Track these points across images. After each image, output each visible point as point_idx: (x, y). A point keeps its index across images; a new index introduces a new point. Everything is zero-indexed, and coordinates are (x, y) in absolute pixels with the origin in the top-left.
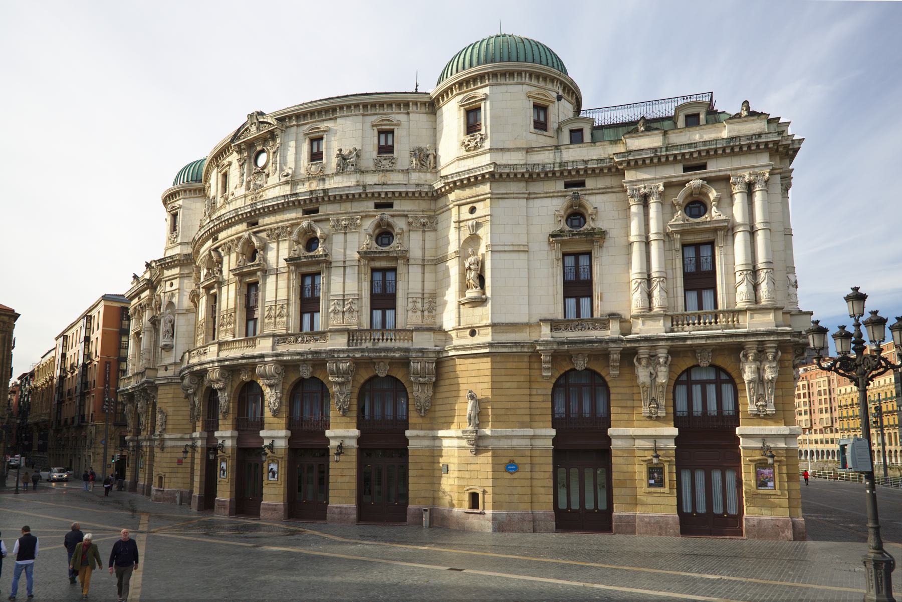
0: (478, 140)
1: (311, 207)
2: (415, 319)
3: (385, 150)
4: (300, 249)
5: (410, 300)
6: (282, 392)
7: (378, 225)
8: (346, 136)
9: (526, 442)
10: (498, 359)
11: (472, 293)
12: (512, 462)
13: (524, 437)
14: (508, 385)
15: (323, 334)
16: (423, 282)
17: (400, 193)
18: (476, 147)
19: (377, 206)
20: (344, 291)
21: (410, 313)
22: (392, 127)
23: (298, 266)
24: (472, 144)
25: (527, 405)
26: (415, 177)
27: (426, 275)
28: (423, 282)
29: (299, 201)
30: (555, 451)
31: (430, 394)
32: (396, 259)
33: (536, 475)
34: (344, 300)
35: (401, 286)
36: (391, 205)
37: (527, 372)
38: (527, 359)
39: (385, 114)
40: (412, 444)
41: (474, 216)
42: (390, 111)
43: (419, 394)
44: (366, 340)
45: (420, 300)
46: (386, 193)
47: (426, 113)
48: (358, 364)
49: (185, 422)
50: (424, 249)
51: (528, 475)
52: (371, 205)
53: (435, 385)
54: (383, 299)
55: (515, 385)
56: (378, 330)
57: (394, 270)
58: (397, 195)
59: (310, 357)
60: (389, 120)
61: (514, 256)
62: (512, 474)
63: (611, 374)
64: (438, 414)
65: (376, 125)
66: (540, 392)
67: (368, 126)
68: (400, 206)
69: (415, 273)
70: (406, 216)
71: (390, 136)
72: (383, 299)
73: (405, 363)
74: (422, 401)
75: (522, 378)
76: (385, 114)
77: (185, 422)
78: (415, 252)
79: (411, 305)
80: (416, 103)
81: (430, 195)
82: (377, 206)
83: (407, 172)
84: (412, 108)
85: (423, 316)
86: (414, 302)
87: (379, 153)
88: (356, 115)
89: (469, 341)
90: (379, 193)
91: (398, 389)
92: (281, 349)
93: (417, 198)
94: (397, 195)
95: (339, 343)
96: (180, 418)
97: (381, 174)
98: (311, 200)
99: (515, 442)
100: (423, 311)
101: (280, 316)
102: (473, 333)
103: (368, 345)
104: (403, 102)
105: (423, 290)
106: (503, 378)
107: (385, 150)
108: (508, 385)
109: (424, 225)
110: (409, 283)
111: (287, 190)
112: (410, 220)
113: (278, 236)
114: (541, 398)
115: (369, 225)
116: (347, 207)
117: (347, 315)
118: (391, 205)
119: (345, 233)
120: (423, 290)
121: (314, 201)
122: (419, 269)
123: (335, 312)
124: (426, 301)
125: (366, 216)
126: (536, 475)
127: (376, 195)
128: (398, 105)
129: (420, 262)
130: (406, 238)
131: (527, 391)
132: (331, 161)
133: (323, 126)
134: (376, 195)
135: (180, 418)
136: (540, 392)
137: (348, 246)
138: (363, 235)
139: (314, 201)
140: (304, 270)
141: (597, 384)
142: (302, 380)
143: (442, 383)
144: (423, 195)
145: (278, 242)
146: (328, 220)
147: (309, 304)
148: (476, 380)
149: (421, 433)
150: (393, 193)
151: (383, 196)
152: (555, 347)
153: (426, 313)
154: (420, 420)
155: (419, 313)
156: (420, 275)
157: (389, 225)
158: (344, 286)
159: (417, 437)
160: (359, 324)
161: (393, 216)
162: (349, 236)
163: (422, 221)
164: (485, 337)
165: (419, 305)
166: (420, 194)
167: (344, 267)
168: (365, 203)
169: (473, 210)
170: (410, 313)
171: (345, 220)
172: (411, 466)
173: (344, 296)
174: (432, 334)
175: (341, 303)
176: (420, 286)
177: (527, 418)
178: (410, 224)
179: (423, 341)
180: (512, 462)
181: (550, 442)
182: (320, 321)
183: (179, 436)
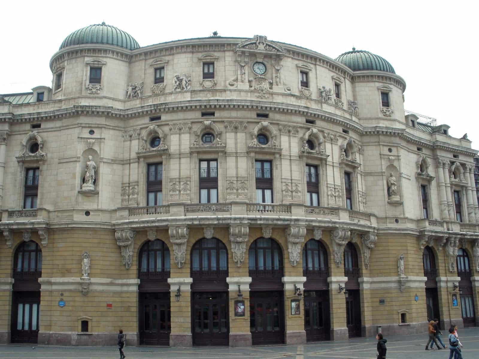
0: (390, 112)
1: (311, 119)
49: (113, 267)
65: (335, 79)
76: (336, 73)
77: (113, 267)
88: (326, 68)
89: (394, 226)
96: (108, 263)
97: (342, 112)
102: (397, 221)
110: (360, 185)
119: (332, 144)
135: (108, 263)
148: (399, 248)
169: (390, 150)
175: (333, 190)
183: (108, 280)
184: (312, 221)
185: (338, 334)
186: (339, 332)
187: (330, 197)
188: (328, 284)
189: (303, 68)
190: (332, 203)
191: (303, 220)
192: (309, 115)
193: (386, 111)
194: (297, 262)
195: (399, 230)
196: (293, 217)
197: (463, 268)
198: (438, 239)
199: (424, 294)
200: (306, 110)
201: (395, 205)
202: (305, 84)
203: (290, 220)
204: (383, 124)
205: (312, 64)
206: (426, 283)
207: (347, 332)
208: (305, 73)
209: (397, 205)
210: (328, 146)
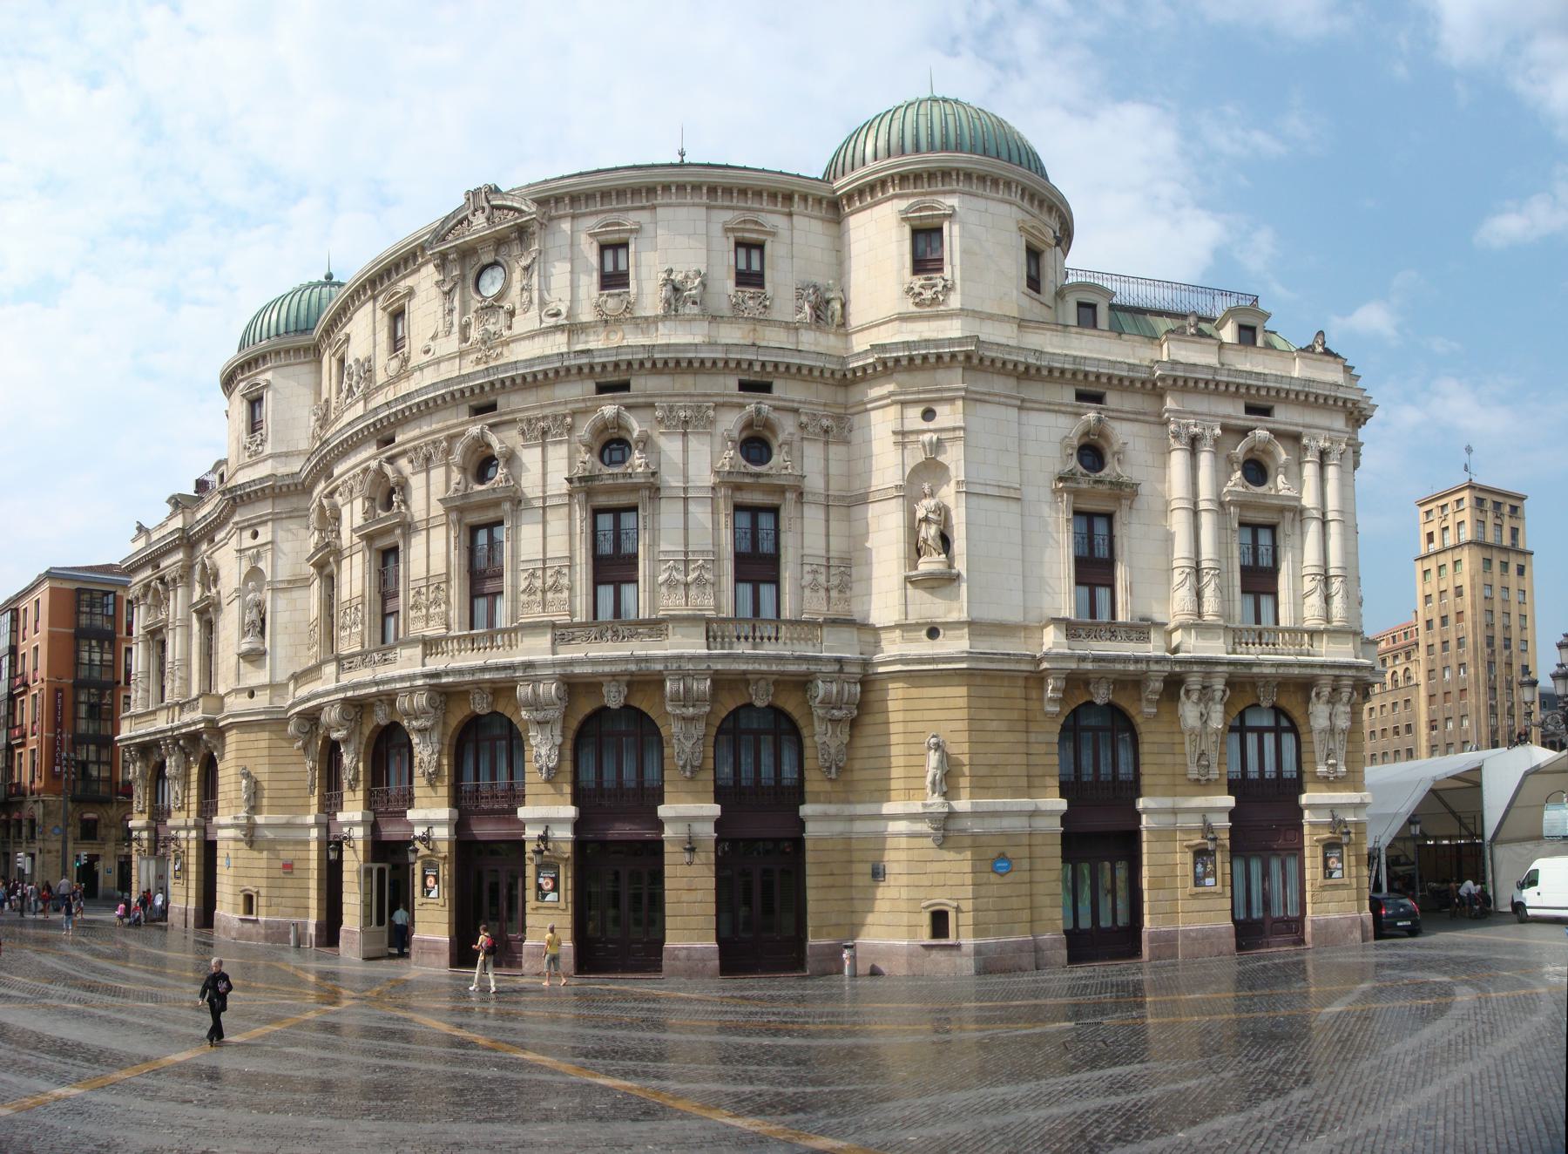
0: (940, 288)
2: (816, 606)
3: (749, 279)
4: (586, 460)
5: (807, 568)
6: (563, 735)
7: (749, 425)
8: (676, 247)
9: (1019, 824)
10: (978, 681)
11: (931, 563)
12: (1002, 857)
13: (1019, 813)
14: (994, 725)
15: (656, 626)
16: (828, 535)
17: (788, 367)
18: (934, 301)
19: (744, 386)
20: (686, 545)
21: (807, 592)
22: (762, 237)
23: (589, 493)
24: (928, 294)
25: (1022, 759)
26: (809, 340)
27: (833, 524)
28: (828, 535)
29: (592, 367)
30: (1063, 835)
31: (846, 739)
32: (782, 490)
33: (1038, 876)
34: (686, 562)
35: (787, 540)
36: (766, 388)
37: (1022, 704)
38: (1021, 683)
39: (749, 209)
40: (812, 830)
41: (931, 425)
42: (756, 205)
43: (821, 738)
44: (738, 638)
45: (823, 570)
46: (763, 364)
47: (822, 219)
48: (722, 682)
50: (827, 475)
51: (1026, 876)
52: (732, 383)
53: (854, 724)
54: (757, 565)
55: (1003, 726)
56: (770, 621)
57: (775, 511)
58: (782, 369)
59: (633, 667)
60: (756, 223)
61: (1002, 504)
62: (1002, 875)
63: (1143, 711)
64: (857, 776)
65: (733, 230)
66: (1041, 738)
67: (717, 229)
68: (784, 390)
69: (813, 517)
70: (796, 411)
71: (755, 255)
72: (757, 565)
73: (802, 683)
74: (833, 751)
75: (1015, 715)
76: (749, 209)
78: (814, 483)
79: (808, 578)
80: (804, 198)
81: (838, 376)
82: (744, 386)
83: (792, 327)
84: (797, 206)
85: (829, 599)
86: (815, 572)
87: (738, 284)
89: (922, 647)
90: (751, 364)
91: (784, 728)
92: (566, 653)
93: (814, 381)
94: (782, 369)
95: (687, 644)
98: (617, 365)
99: (1006, 824)
100: (827, 590)
101: (556, 588)
103: (743, 648)
104: (783, 193)
105: (828, 551)
106: (987, 714)
107: (749, 279)
108: (994, 725)
109: (826, 431)
110: (804, 538)
111: (557, 344)
112: (804, 419)
113: (544, 433)
114: (1042, 749)
115: (730, 422)
116: (688, 383)
117: (693, 592)
118: (766, 388)
119: (685, 434)
120: (828, 551)
121: (623, 366)
122: (821, 514)
123: (671, 584)
124: (833, 571)
125: (723, 405)
126: (1038, 876)
127: (745, 366)
128: (773, 196)
129: (822, 499)
130: (796, 453)
131: (1022, 737)
132: (647, 291)
133: (631, 219)
134: (745, 366)
136: (1041, 738)
137: (694, 461)
138: (718, 440)
139: (623, 366)
140: (602, 501)
141: (1119, 723)
142: (602, 712)
143: (867, 719)
144: (827, 374)
145: (544, 446)
146: (652, 406)
147: (613, 567)
149: (832, 809)
150: (776, 365)
151: (757, 368)
152: (1073, 666)
153: (834, 594)
154: (827, 786)
155: (822, 593)
156: (822, 523)
157: (768, 425)
158: (685, 538)
159: (826, 817)
160: (718, 608)
161: (776, 408)
162: (693, 442)
163: (825, 422)
164: (955, 644)
165: (822, 579)
166: (822, 372)
167: (686, 499)
168: (721, 379)
169: (928, 415)
170: (807, 592)
171: (685, 408)
172: (809, 869)
173: (686, 553)
174: (855, 632)
175: (682, 567)
176: (822, 544)
177: (1023, 782)
178: (802, 427)
179: (835, 645)
180: (1002, 857)
181: (1058, 821)
182: (639, 600)
184: (572, 662)
185: (676, 958)
186: (683, 954)
187: (664, 589)
188: (659, 824)
189: (607, 232)
190: (672, 603)
191: (545, 665)
192: (598, 369)
193: (922, 287)
194: (548, 769)
195: (933, 660)
196: (518, 659)
197: (1270, 765)
198: (1132, 683)
199: (1058, 850)
200: (584, 360)
201: (928, 584)
202: (613, 280)
203: (511, 667)
204: (912, 332)
205: (643, 208)
206: (1065, 818)
207: (716, 956)
208: (613, 247)
209: (935, 584)
210: (671, 447)
